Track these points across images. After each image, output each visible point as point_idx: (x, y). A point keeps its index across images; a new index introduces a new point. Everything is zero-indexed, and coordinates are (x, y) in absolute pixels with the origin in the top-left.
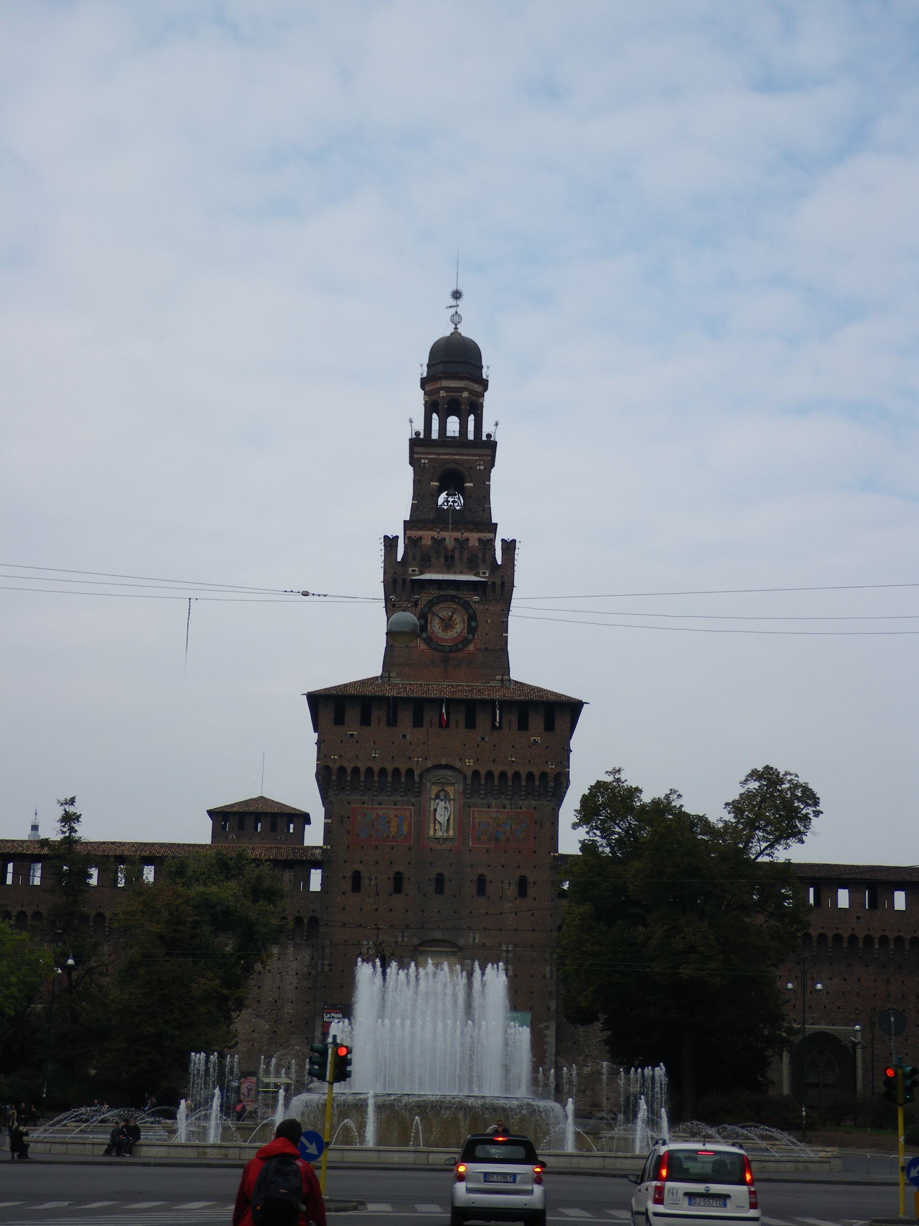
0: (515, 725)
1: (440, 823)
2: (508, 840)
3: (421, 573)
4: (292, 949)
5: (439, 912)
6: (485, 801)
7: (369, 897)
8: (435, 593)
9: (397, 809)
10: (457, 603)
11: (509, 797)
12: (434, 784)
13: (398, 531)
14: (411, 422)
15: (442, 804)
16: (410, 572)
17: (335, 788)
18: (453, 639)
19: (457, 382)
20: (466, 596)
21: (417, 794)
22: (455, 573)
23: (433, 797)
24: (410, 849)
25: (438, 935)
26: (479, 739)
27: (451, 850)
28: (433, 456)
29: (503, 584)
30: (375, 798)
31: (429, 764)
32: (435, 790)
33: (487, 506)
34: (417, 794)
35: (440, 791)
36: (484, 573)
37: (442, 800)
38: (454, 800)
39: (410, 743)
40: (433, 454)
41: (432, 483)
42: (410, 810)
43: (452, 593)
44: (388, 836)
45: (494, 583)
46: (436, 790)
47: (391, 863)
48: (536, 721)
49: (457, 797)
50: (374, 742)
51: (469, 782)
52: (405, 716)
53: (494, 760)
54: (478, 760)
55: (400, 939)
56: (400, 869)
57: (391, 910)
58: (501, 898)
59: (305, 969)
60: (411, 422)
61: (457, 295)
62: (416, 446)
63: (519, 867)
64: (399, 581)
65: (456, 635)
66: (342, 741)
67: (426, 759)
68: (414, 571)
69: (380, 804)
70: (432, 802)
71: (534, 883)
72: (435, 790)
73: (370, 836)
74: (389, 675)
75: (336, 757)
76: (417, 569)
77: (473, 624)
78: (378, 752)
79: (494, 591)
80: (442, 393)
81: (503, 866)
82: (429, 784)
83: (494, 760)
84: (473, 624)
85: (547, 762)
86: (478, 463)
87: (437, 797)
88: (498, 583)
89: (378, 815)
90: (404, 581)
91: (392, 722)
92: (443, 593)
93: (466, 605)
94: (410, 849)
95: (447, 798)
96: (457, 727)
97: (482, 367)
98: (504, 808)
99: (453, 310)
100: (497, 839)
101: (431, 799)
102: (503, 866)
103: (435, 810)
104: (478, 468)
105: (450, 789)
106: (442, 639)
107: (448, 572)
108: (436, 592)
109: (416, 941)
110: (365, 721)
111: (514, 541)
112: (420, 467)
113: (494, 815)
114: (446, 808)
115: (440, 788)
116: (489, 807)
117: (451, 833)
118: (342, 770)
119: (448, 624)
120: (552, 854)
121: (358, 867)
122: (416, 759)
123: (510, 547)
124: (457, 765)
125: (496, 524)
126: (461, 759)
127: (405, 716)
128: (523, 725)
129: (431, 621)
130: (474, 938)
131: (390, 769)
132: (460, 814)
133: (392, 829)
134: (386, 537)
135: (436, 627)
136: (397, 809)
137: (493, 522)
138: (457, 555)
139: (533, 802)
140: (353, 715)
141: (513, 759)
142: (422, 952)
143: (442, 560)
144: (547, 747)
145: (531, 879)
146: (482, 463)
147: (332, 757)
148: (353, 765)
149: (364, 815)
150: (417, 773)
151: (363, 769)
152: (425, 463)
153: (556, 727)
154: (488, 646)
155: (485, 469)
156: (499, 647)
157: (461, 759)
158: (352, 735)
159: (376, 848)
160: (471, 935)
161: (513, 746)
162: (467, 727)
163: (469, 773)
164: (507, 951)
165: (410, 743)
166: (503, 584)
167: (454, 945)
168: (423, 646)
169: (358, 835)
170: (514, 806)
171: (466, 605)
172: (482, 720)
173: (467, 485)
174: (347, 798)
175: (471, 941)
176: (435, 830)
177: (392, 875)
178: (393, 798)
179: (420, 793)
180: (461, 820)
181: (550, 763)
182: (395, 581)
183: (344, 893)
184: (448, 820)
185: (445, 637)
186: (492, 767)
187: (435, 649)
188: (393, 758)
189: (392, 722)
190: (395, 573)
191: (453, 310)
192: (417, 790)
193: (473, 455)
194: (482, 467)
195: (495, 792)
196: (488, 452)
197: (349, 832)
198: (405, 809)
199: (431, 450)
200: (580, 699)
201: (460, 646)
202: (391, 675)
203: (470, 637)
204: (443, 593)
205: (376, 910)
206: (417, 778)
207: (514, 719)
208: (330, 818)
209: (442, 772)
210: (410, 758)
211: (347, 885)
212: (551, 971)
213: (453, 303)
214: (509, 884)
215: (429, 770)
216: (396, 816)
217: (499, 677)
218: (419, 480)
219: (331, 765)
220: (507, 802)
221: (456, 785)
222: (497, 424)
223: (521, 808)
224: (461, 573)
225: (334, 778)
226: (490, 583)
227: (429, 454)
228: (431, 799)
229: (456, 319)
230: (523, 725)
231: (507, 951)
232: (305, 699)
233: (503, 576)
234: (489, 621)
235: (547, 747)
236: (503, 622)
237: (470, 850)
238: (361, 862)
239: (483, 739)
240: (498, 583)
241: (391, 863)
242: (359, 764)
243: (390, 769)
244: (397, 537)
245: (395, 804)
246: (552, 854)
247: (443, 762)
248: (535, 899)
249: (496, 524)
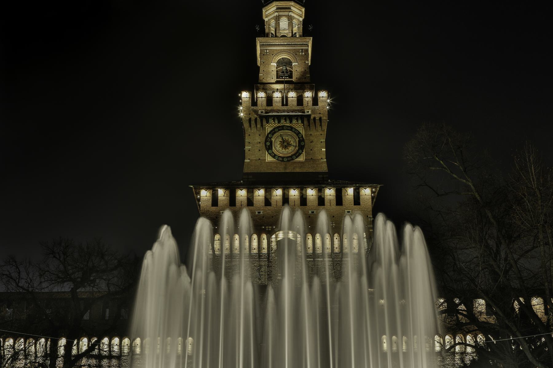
20: (297, 127)
26: (310, 212)
29: (320, 119)
36: (308, 112)
45: (314, 118)
77: (302, 144)
88: (317, 118)
119: (285, 144)
135: (277, 148)
155: (305, 54)
166: (320, 119)
194: (303, 53)
226: (312, 118)
240: (317, 118)
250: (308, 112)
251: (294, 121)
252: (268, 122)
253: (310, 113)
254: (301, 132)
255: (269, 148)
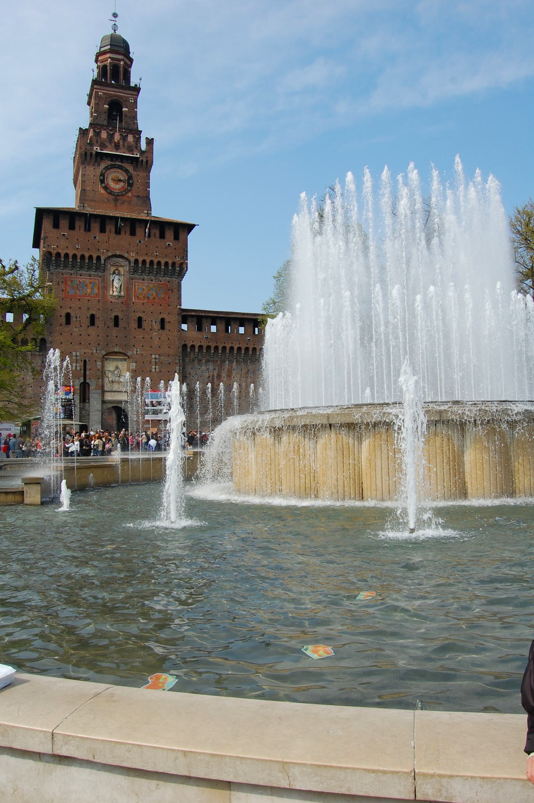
0: (158, 235)
1: (116, 287)
2: (154, 298)
3: (101, 150)
4: (30, 356)
5: (117, 336)
6: (141, 277)
7: (76, 328)
8: (109, 163)
9: (91, 279)
10: (122, 170)
11: (155, 275)
12: (112, 265)
13: (86, 126)
14: (93, 71)
15: (117, 277)
16: (95, 149)
17: (54, 265)
18: (119, 189)
19: (118, 56)
21: (103, 271)
22: (121, 153)
23: (112, 273)
24: (99, 301)
25: (116, 349)
26: (138, 241)
27: (122, 303)
28: (106, 92)
29: (147, 161)
30: (78, 272)
31: (110, 254)
32: (113, 269)
33: (135, 122)
34: (103, 271)
35: (116, 270)
37: (117, 275)
38: (124, 275)
39: (99, 242)
40: (105, 90)
41: (105, 106)
42: (99, 280)
43: (118, 163)
44: (86, 294)
45: (142, 160)
46: (114, 269)
47: (88, 309)
48: (169, 234)
49: (125, 273)
50: (77, 240)
51: (132, 265)
52: (95, 226)
53: (147, 254)
54: (137, 253)
55: (95, 351)
56: (94, 313)
57: (89, 335)
58: (151, 330)
59: (39, 368)
60: (93, 71)
61: (115, 15)
62: (96, 84)
63: (160, 313)
64: (89, 154)
65: (121, 187)
66: (58, 238)
67: (108, 251)
68: (97, 149)
69: (81, 275)
70: (111, 276)
71: (169, 322)
72: (113, 269)
73: (76, 293)
74: (83, 205)
75: (55, 247)
76: (98, 148)
78: (79, 245)
79: (142, 165)
80: (109, 60)
81: (152, 313)
82: (109, 265)
83: (147, 254)
84: (131, 181)
85: (175, 257)
86: (130, 98)
87: (114, 273)
88: (145, 160)
89: (80, 282)
90: (91, 154)
91: (88, 229)
92: (113, 163)
93: (126, 171)
94: (99, 301)
95: (119, 274)
96: (125, 234)
97: (130, 53)
98: (152, 281)
99: (114, 23)
100: (148, 298)
101: (111, 274)
102: (152, 313)
103: (113, 280)
104: (131, 101)
105: (121, 269)
106: (113, 188)
107: (116, 151)
108: (109, 162)
109: (104, 353)
110: (72, 227)
111: (153, 139)
112: (98, 96)
113: (147, 284)
114: (119, 279)
115: (116, 268)
116: (143, 280)
117: (122, 293)
118: (58, 255)
120: (178, 307)
121: (69, 311)
122: (102, 251)
123: (150, 142)
124: (126, 255)
125: (141, 131)
126: (128, 252)
127: (95, 226)
128: (162, 236)
129: (107, 179)
130: (137, 351)
131: (87, 255)
132: (127, 283)
133: (88, 290)
134: (80, 129)
136: (91, 279)
137: (139, 129)
138: (121, 143)
139: (167, 278)
140: (64, 223)
141: (157, 254)
142: (106, 359)
143: (113, 145)
144: (175, 249)
145: (167, 320)
146: (132, 99)
147: (52, 246)
148: (65, 252)
149: (72, 282)
150: (102, 258)
151: (71, 255)
152: (101, 95)
153: (180, 238)
154: (139, 194)
156: (145, 196)
157: (128, 252)
158: (64, 235)
159: (79, 300)
160: (135, 349)
161: (157, 247)
162: (130, 235)
163: (132, 260)
164: (156, 359)
165: (99, 242)
166: (147, 161)
167: (126, 355)
168: (102, 191)
169: (68, 292)
170: (157, 280)
171: (126, 171)
172: (139, 231)
173: (124, 109)
174: (62, 271)
175: (135, 352)
176: (113, 291)
177: (89, 316)
178: (88, 273)
179: (104, 271)
180: (128, 288)
181: (177, 257)
182: (86, 154)
183: (61, 325)
184: (121, 286)
185: (115, 188)
186: (145, 258)
187: (109, 193)
188: (88, 249)
189: (88, 229)
190: (86, 149)
191: (114, 23)
192: (103, 268)
193: (127, 94)
194: (133, 101)
195: (147, 272)
196: (136, 93)
197: (63, 291)
198: (96, 279)
199: (104, 88)
200: (194, 223)
201: (124, 193)
202: (86, 205)
203: (129, 188)
204: (113, 163)
205: (80, 335)
206: (103, 262)
207: (157, 232)
208: (51, 282)
209: (116, 259)
210: (98, 250)
211: (63, 320)
212: (180, 369)
213: (114, 19)
214: (156, 322)
215: (109, 258)
216: (90, 283)
217: (146, 212)
218: (97, 103)
219: (52, 251)
220: (153, 278)
221: (124, 267)
222: (141, 79)
223: (161, 281)
224: (124, 153)
225: (54, 258)
226: (141, 159)
227: (103, 90)
228: (111, 274)
229: (115, 29)
230: (162, 236)
231: (156, 359)
232: (35, 211)
233: (147, 157)
234: (139, 181)
235: (175, 249)
236: (147, 182)
237: (133, 303)
238: (71, 308)
239: (140, 242)
240: (145, 160)
241: (88, 309)
242: (68, 252)
243: (87, 255)
244: (86, 130)
245: (90, 276)
246: (178, 307)
247: (118, 253)
248: (169, 330)
249: (141, 131)
250: (137, 154)
251: (124, 161)
252: (102, 159)
253: (138, 156)
254: (130, 171)
255: (102, 181)
